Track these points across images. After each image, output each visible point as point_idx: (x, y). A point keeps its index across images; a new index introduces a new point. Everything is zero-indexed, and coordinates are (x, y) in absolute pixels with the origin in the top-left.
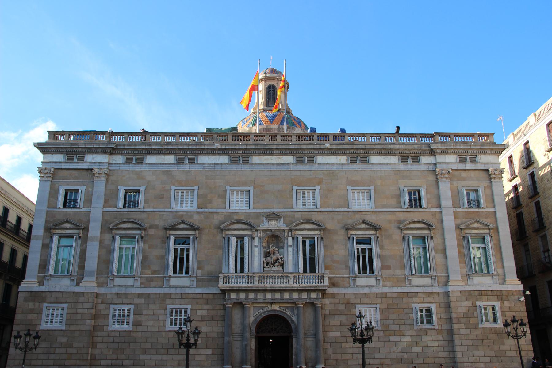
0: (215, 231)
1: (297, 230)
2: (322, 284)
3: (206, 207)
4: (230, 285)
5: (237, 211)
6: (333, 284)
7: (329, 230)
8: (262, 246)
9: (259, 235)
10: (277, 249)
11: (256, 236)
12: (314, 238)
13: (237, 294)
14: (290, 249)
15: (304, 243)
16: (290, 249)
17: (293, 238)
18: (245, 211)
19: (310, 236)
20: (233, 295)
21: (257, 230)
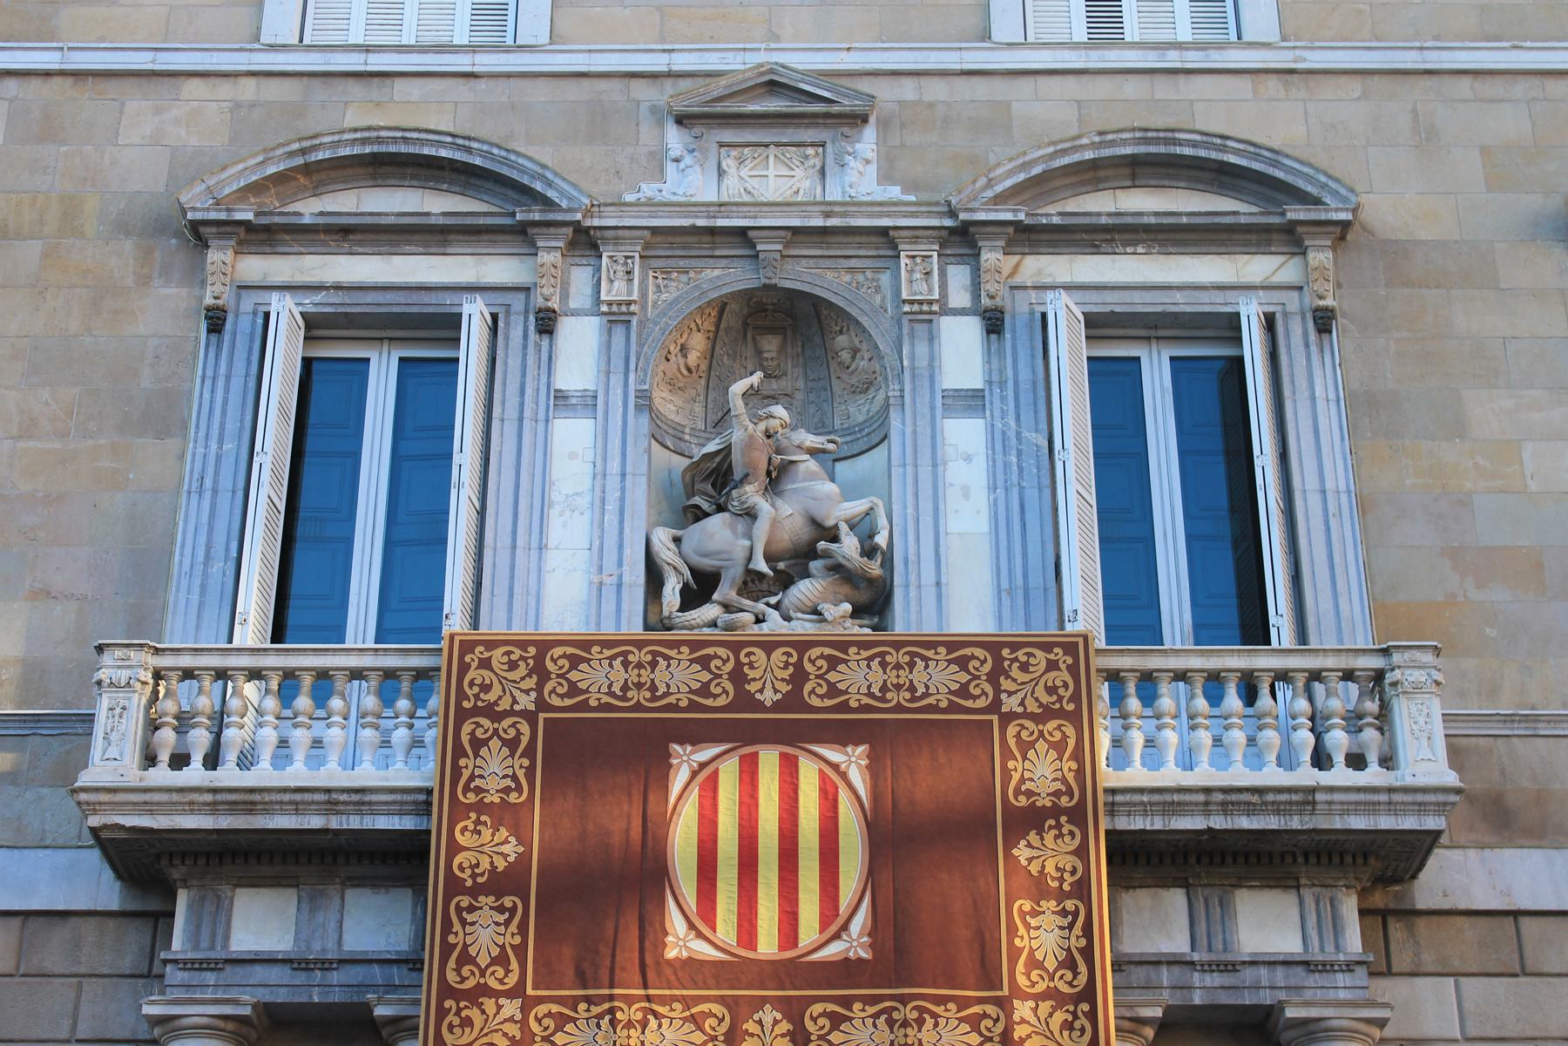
0: (121, 259)
1: (1028, 237)
2: (1373, 775)
3: (44, 34)
4: (229, 775)
5: (378, 62)
6: (1501, 816)
7: (1396, 257)
8: (645, 402)
9: (615, 290)
10: (811, 440)
11: (580, 294)
12: (1230, 326)
13: (311, 904)
14: (965, 435)
15: (1114, 387)
16: (965, 435)
17: (994, 323)
18: (461, 63)
19: (1182, 303)
20: (261, 923)
21: (585, 241)
